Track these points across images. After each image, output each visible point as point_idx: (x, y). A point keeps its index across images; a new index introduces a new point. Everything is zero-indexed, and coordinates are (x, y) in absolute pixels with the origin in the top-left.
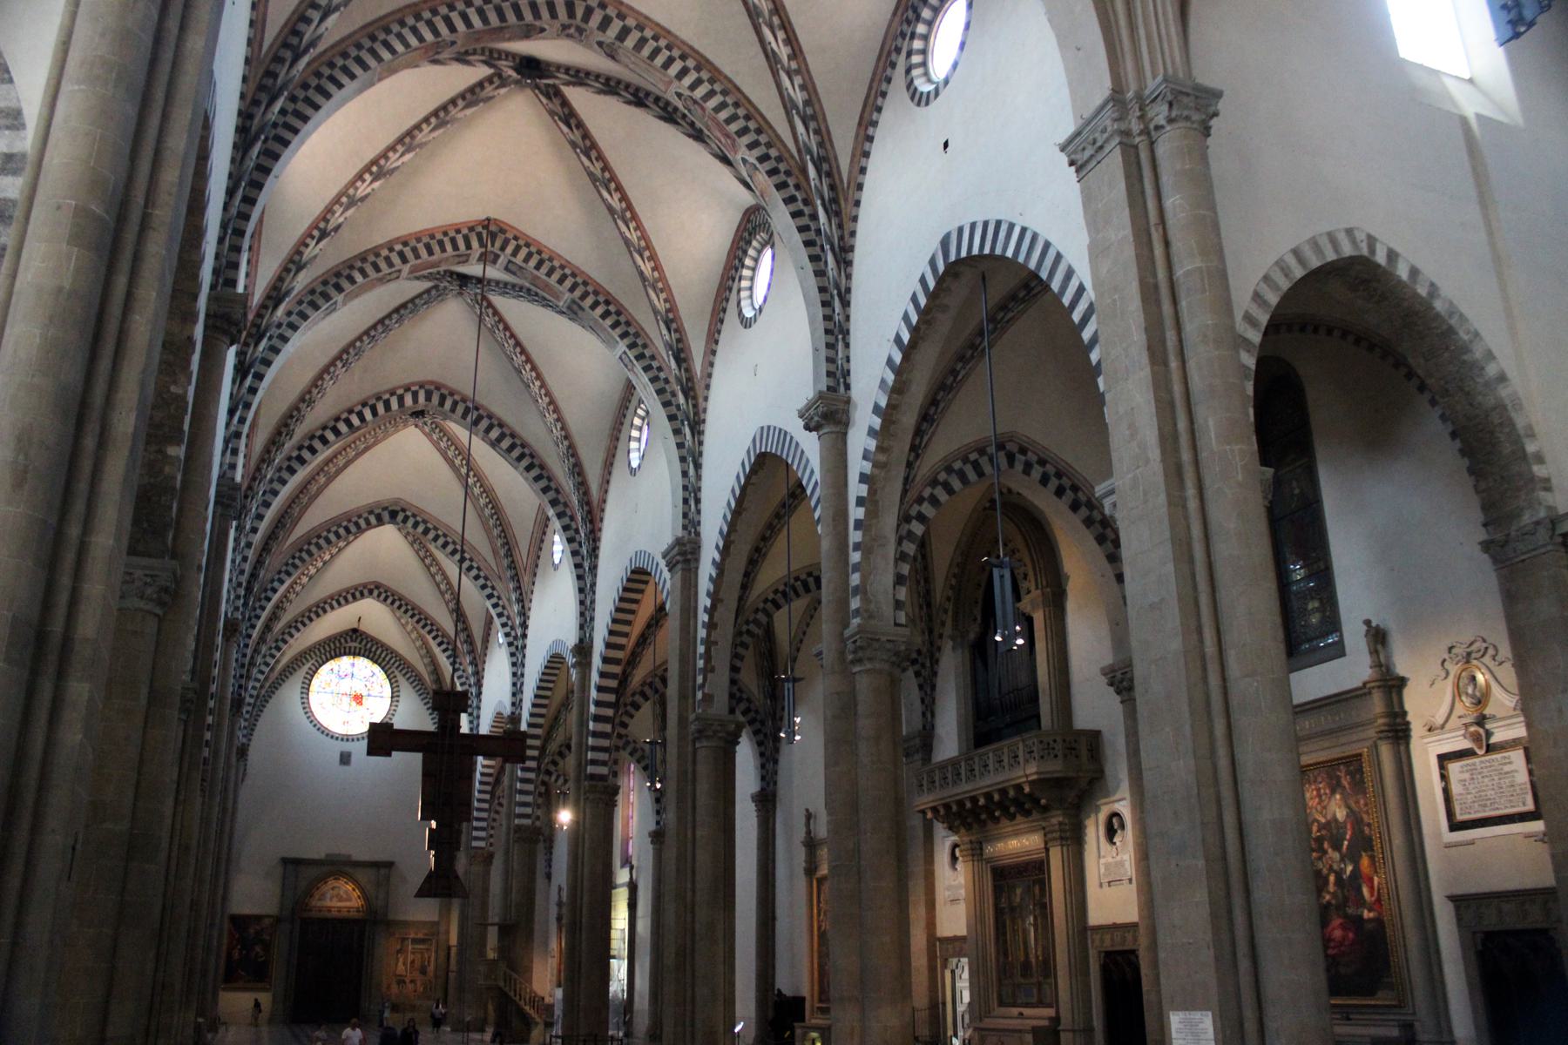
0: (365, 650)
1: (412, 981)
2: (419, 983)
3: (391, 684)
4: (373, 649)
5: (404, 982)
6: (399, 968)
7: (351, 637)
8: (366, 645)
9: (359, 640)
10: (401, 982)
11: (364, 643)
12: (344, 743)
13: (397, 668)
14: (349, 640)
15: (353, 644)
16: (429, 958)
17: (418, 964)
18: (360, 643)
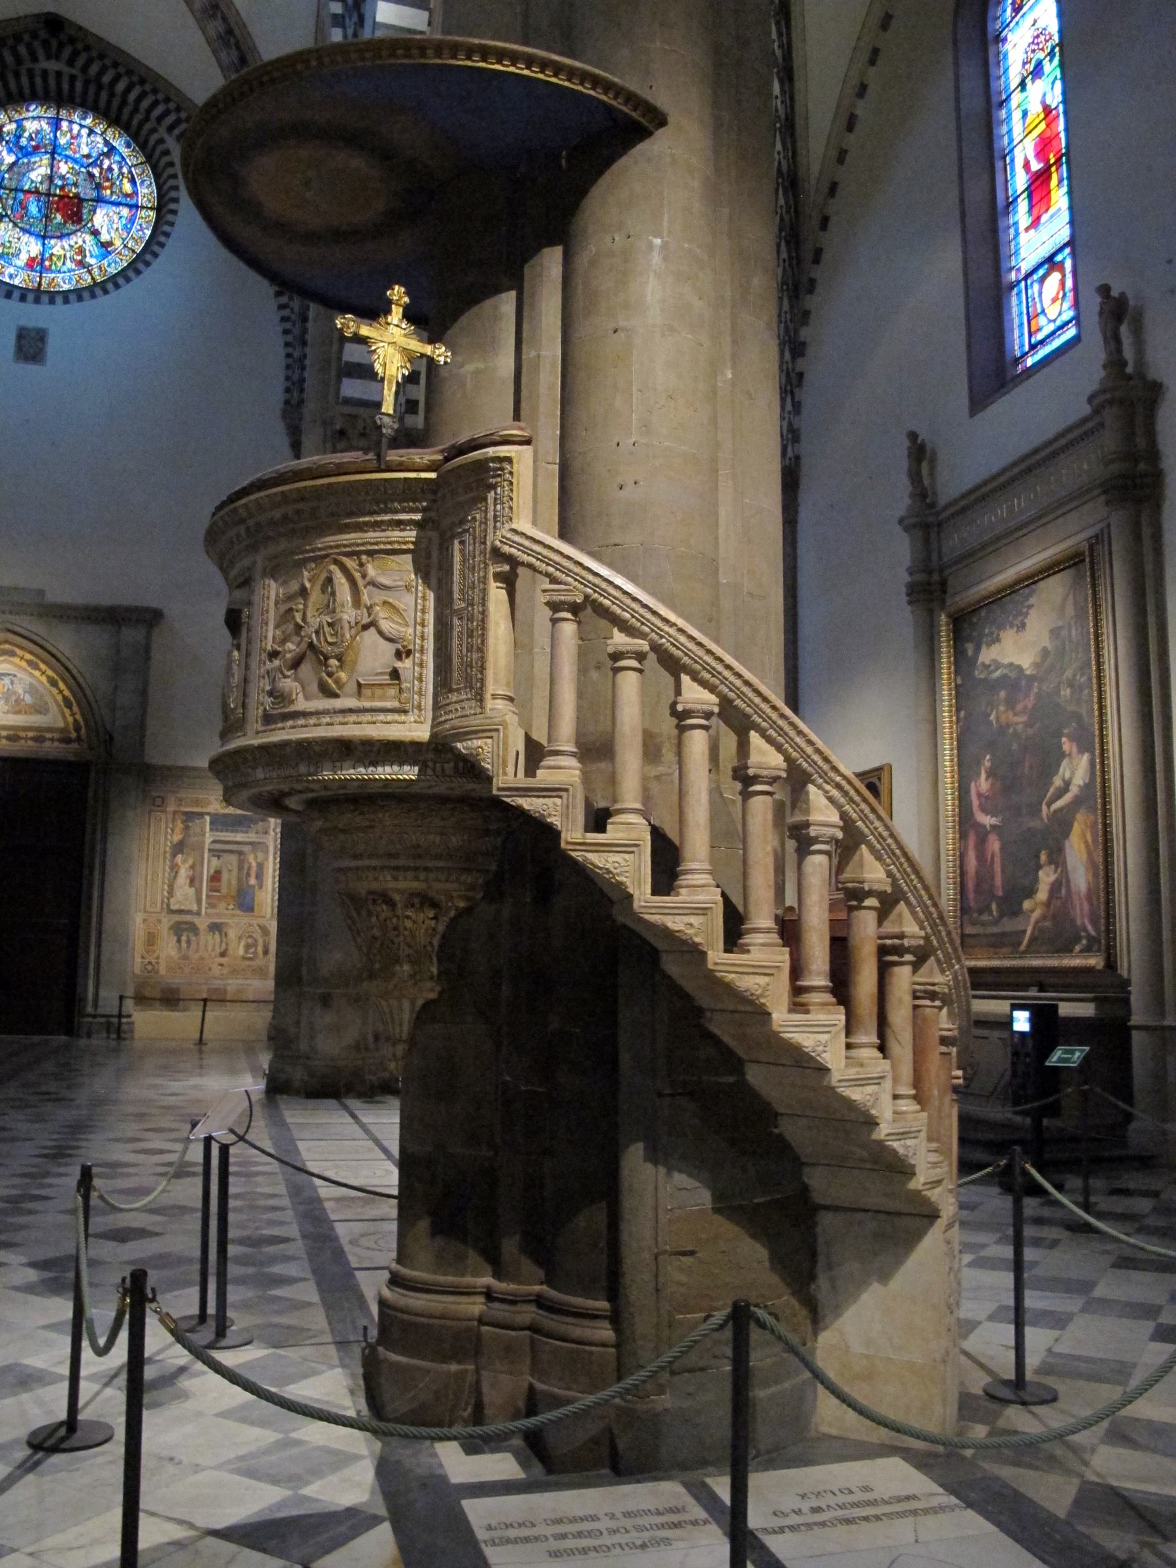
0: (87, 82)
1: (215, 928)
2: (232, 934)
3: (157, 176)
4: (106, 79)
5: (193, 929)
6: (178, 893)
7: (46, 44)
8: (85, 69)
9: (67, 52)
10: (183, 929)
11: (80, 61)
12: (29, 307)
13: (171, 129)
14: (41, 53)
15: (52, 66)
16: (260, 866)
17: (229, 879)
18: (71, 62)
